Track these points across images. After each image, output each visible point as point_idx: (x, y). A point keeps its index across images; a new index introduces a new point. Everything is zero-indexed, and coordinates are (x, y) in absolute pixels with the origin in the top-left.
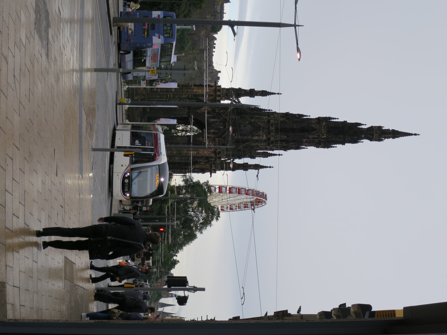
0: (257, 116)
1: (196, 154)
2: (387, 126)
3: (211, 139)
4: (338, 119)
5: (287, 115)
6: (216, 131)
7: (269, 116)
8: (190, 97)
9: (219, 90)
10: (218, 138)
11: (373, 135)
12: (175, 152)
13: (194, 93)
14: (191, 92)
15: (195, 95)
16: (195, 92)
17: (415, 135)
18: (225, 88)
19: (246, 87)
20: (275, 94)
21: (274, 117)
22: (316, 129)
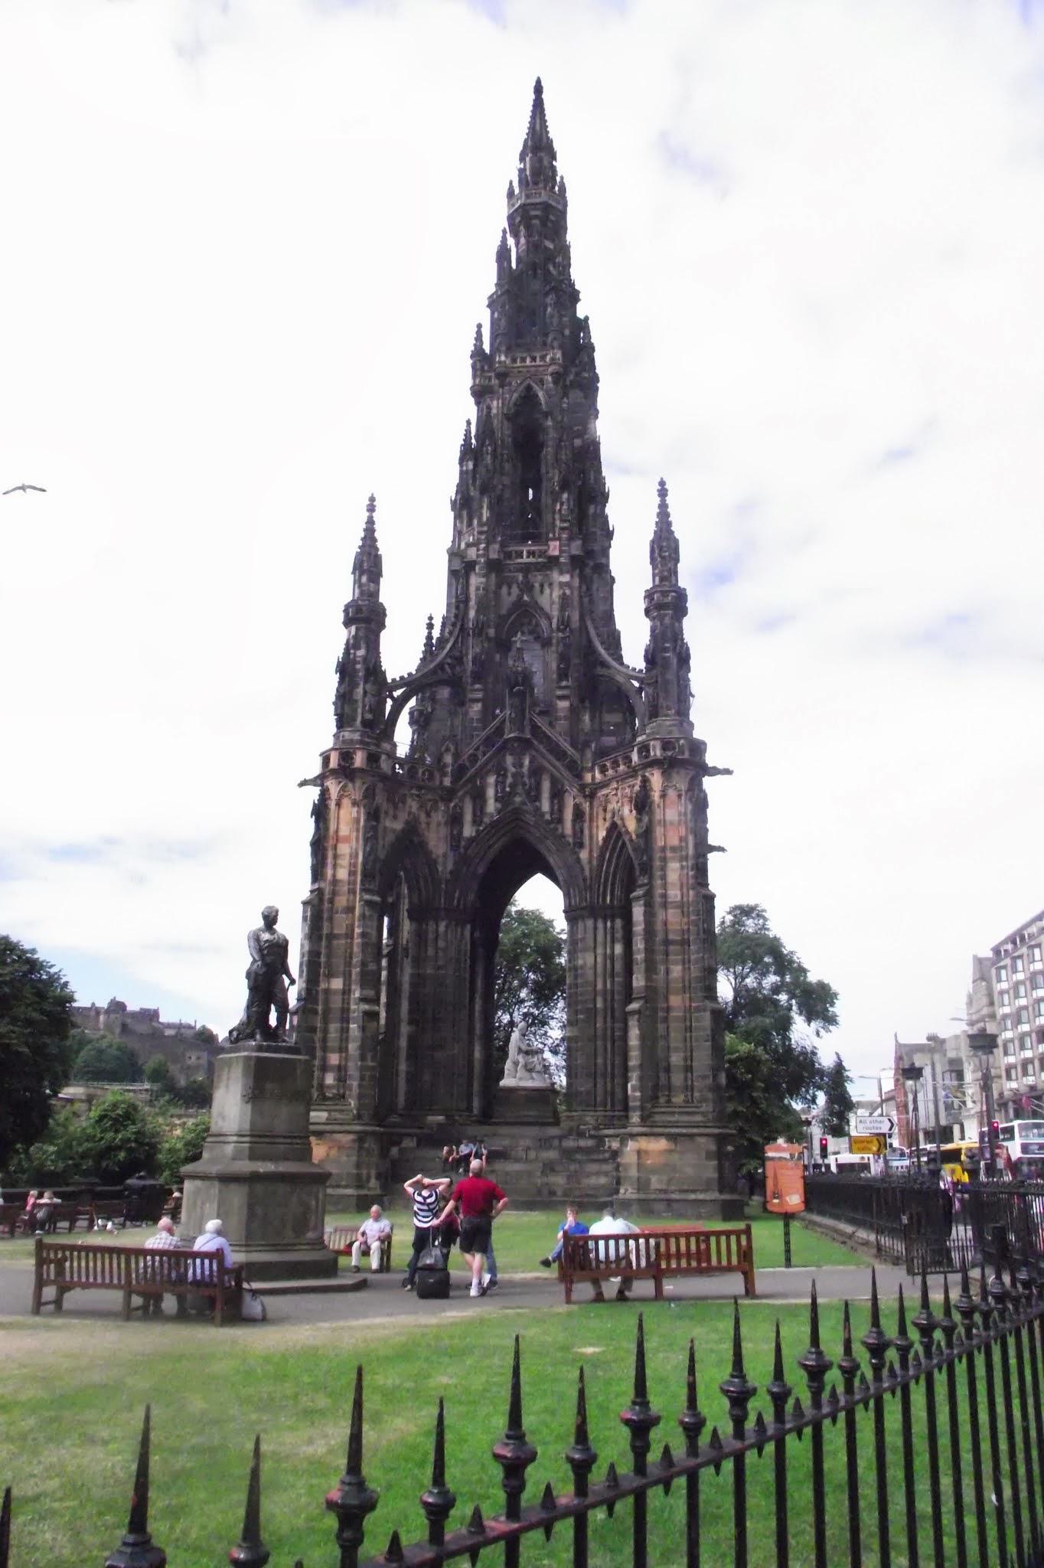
0: (472, 614)
2: (508, 167)
3: (586, 806)
4: (479, 326)
5: (463, 505)
6: (546, 786)
7: (470, 566)
8: (377, 898)
9: (346, 756)
10: (579, 776)
12: (676, 971)
14: (352, 892)
16: (352, 873)
17: (538, 89)
19: (336, 638)
20: (370, 522)
21: (475, 544)
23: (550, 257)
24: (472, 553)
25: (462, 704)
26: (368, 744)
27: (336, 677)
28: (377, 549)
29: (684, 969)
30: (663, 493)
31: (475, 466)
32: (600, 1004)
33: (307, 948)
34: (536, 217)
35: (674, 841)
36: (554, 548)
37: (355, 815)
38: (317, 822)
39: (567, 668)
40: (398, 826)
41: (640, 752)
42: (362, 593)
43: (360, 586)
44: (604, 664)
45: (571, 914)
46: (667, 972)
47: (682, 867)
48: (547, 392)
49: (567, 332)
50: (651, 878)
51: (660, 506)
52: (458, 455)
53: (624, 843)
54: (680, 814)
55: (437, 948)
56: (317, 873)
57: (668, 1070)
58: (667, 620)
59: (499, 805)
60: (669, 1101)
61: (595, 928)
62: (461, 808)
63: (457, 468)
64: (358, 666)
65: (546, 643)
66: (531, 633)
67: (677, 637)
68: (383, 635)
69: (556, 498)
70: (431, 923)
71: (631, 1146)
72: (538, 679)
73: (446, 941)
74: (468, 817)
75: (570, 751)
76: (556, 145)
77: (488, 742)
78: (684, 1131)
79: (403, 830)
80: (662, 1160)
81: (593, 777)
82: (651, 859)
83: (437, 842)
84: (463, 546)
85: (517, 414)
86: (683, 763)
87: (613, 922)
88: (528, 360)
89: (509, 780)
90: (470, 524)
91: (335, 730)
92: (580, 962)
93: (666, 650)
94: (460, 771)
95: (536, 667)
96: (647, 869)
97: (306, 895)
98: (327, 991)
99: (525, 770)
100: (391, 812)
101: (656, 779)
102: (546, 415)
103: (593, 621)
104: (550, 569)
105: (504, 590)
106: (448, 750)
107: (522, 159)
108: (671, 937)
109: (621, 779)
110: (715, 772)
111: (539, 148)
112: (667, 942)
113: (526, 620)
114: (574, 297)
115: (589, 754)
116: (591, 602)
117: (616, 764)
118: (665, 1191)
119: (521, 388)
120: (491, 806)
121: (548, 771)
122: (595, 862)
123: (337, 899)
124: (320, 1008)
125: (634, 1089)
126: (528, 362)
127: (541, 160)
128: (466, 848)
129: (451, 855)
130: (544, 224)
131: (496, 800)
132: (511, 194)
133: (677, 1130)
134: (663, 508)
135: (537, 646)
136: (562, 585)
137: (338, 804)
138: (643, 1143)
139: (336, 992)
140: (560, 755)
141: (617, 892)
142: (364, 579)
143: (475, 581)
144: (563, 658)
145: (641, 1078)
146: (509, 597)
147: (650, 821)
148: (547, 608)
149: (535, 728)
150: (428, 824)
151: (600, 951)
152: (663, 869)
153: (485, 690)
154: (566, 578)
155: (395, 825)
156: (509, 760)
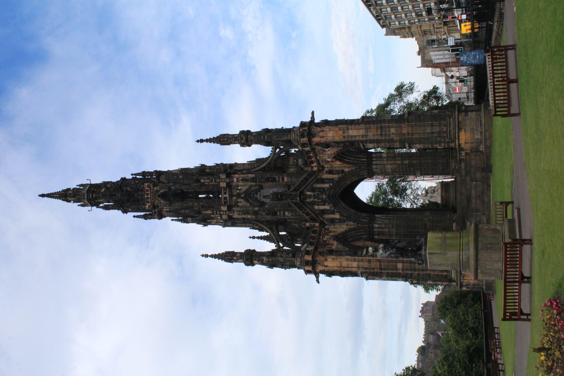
0: (249, 217)
1: (348, 129)
2: (73, 207)
4: (134, 217)
5: (205, 221)
6: (318, 186)
7: (230, 218)
9: (307, 263)
10: (315, 172)
11: (88, 191)
12: (393, 130)
13: (356, 258)
14: (362, 260)
15: (355, 254)
16: (355, 260)
17: (43, 196)
18: (299, 268)
19: (259, 269)
20: (212, 256)
21: (221, 215)
22: (159, 196)
23: (108, 189)
24: (225, 217)
25: (285, 220)
26: (302, 255)
27: (275, 269)
28: (223, 253)
29: (392, 127)
30: (202, 141)
31: (190, 217)
32: (407, 162)
33: (385, 278)
34: (92, 195)
35: (341, 132)
36: (223, 185)
37: (331, 260)
38: (334, 275)
39: (272, 178)
40: (335, 243)
41: (305, 147)
42: (241, 258)
43: (238, 259)
44: (269, 164)
45: (371, 175)
46: (393, 134)
47: (351, 129)
48: (162, 188)
49: (137, 182)
50: (355, 141)
51: (207, 142)
52: (185, 224)
53: (342, 153)
54: (330, 130)
55: (384, 228)
56: (354, 274)
57: (432, 133)
58: (252, 138)
59: (327, 204)
60: (445, 132)
61: (376, 164)
62: (328, 219)
63: (190, 224)
64: (270, 260)
65: (261, 187)
66: (257, 194)
67: (258, 133)
68: (257, 250)
69: (203, 184)
70: (375, 230)
71: (463, 146)
72: (275, 190)
73: (382, 224)
74: (332, 216)
75: (305, 176)
76: (65, 188)
77: (300, 208)
78: (456, 124)
79: (337, 241)
80: (468, 134)
81: (315, 166)
82: (348, 141)
83: (341, 228)
84: (222, 221)
85: (169, 200)
86: (309, 129)
87: (374, 158)
88: (149, 196)
89: (316, 200)
90: (213, 218)
91: (296, 269)
92: (390, 170)
93: (264, 137)
94: (313, 220)
95: (271, 191)
96: (352, 143)
97: (364, 279)
98: (403, 270)
99: (312, 194)
100: (329, 246)
101: (316, 140)
102: (170, 189)
103: (252, 169)
104: (231, 186)
105: (240, 204)
106: (304, 225)
107: (69, 201)
108: (379, 133)
109: (316, 156)
110: (313, 118)
111: (66, 195)
112: (381, 135)
113: (252, 195)
114: (123, 179)
115: (306, 169)
116: (245, 170)
117: (310, 157)
118: (481, 132)
119: (159, 199)
120: (327, 207)
121: (312, 185)
122: (349, 166)
123: (365, 266)
124: (410, 272)
125: (440, 146)
126: (149, 196)
127: (70, 194)
128: (344, 216)
129: (346, 223)
130: (95, 192)
131: (324, 205)
132: (83, 206)
133: (457, 129)
134: (207, 141)
135: (262, 191)
136: (238, 181)
137: (327, 266)
138: (462, 142)
139: (403, 266)
140: (306, 179)
141: (361, 156)
142: (235, 258)
143: (236, 216)
144: (267, 180)
145: (436, 143)
146: (242, 202)
147: (334, 142)
148: (247, 187)
149: (295, 190)
150: (334, 232)
151: (385, 162)
152: (352, 136)
153: (280, 211)
154: (235, 180)
155: (335, 245)
156: (308, 200)
